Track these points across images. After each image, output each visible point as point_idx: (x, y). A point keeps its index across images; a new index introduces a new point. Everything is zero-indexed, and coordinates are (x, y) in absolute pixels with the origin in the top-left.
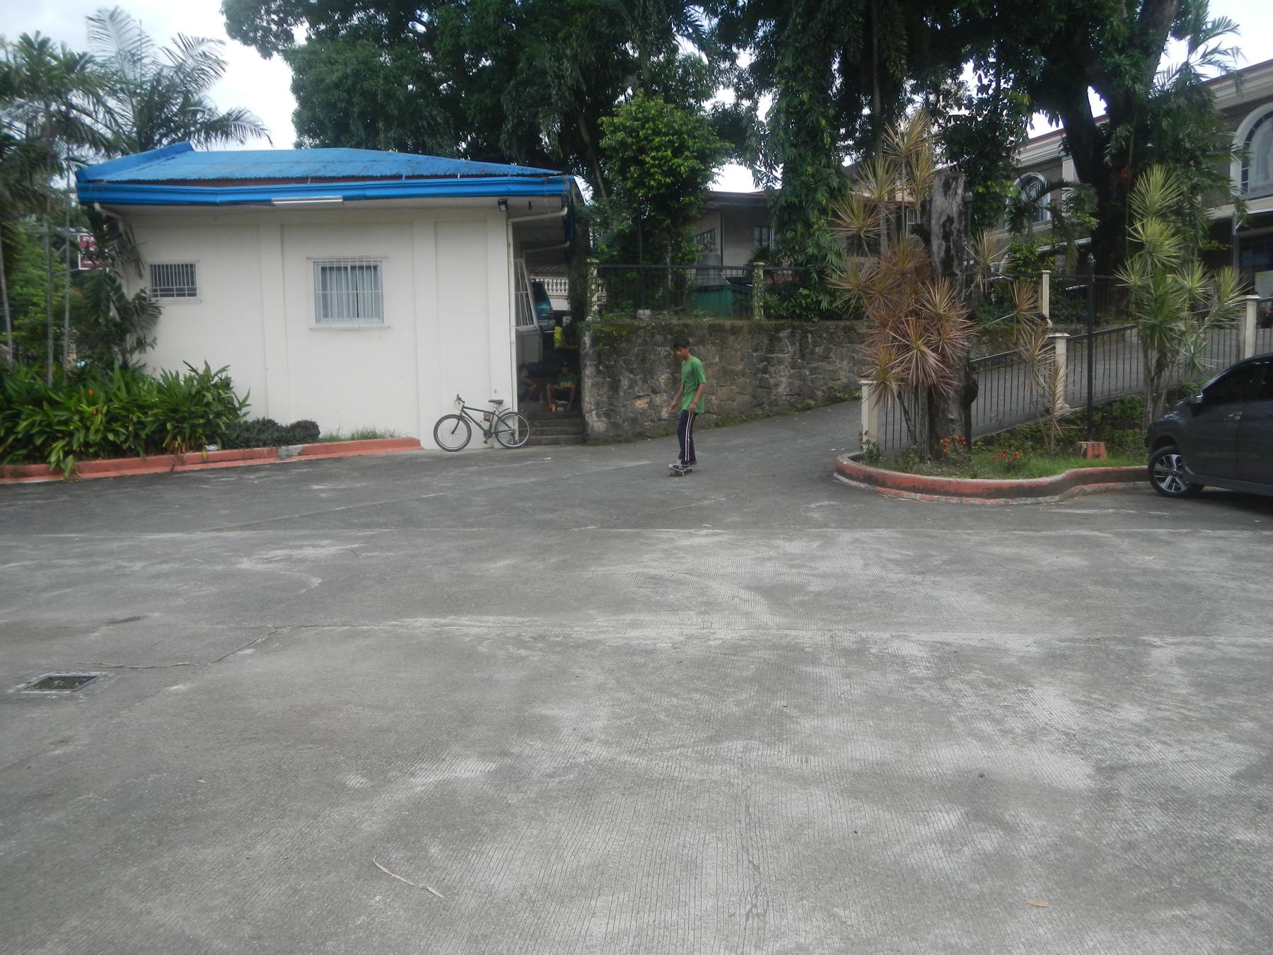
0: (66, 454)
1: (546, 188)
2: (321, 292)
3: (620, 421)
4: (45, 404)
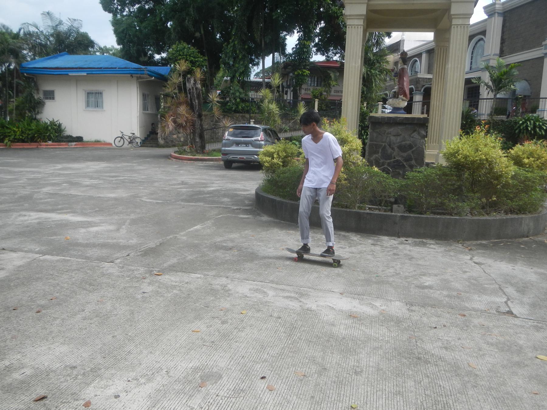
0: (9, 141)
1: (139, 72)
2: (86, 100)
3: (168, 141)
4: (5, 128)
